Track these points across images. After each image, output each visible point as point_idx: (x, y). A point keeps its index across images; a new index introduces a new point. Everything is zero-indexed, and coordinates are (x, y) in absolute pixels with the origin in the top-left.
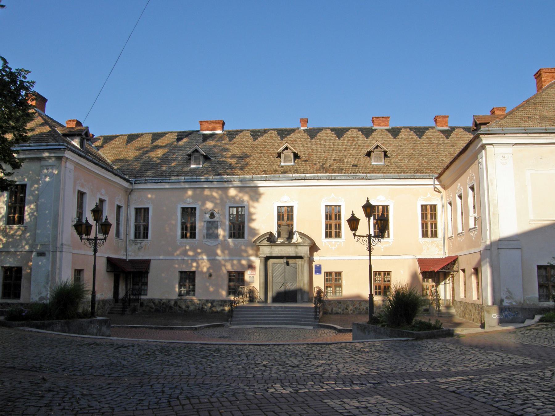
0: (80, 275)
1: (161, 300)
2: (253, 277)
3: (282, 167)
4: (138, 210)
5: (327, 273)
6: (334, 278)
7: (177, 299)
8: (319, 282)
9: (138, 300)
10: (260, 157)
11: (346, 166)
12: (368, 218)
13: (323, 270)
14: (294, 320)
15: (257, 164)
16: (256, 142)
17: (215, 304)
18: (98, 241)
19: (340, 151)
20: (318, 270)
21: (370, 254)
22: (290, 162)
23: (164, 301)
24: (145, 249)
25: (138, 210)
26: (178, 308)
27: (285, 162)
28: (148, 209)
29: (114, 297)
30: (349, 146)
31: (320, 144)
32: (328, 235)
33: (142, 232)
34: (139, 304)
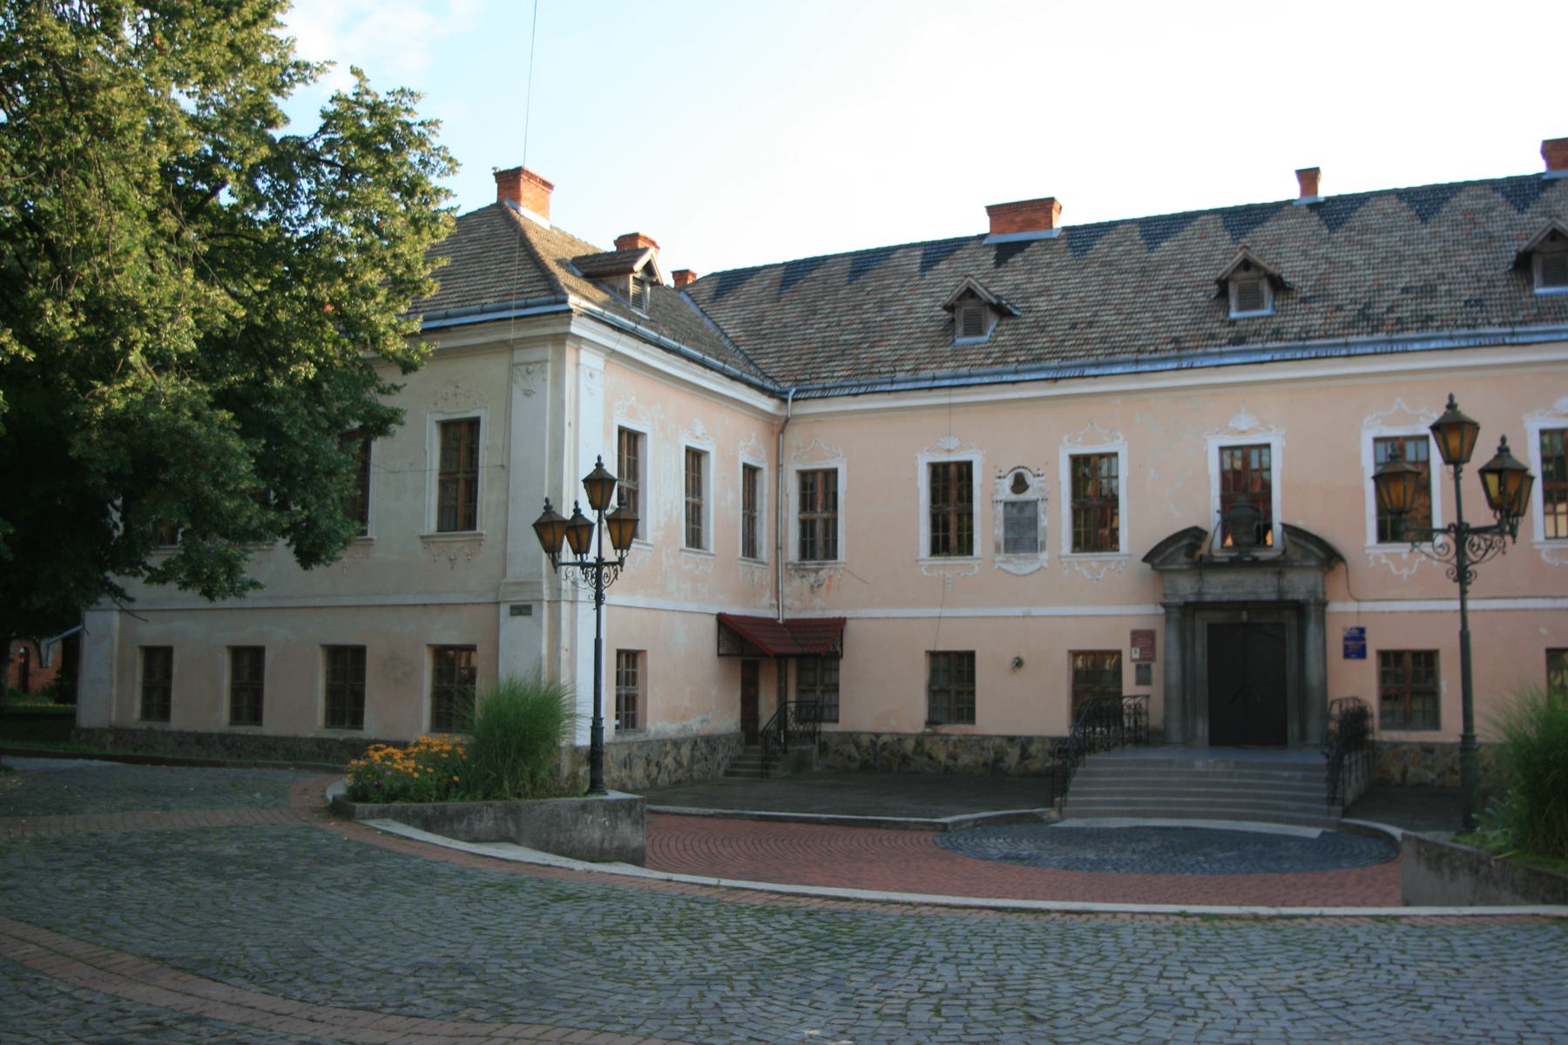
0: (634, 666)
1: (878, 735)
2: (1148, 668)
3: (1233, 323)
4: (807, 479)
5: (1384, 656)
6: (1410, 675)
7: (924, 734)
8: (1357, 683)
9: (812, 736)
10: (1164, 299)
11: (1440, 306)
12: (1451, 468)
13: (1373, 644)
14: (1262, 807)
15: (1157, 319)
16: (1155, 256)
17: (1033, 749)
18: (605, 570)
19: (1425, 261)
20: (1355, 646)
21: (1463, 593)
22: (1258, 305)
23: (885, 738)
24: (829, 587)
25: (807, 479)
26: (926, 759)
27: (1241, 309)
28: (835, 471)
29: (743, 728)
30: (1457, 242)
31: (1360, 243)
32: (1388, 532)
33: (818, 540)
34: (816, 748)
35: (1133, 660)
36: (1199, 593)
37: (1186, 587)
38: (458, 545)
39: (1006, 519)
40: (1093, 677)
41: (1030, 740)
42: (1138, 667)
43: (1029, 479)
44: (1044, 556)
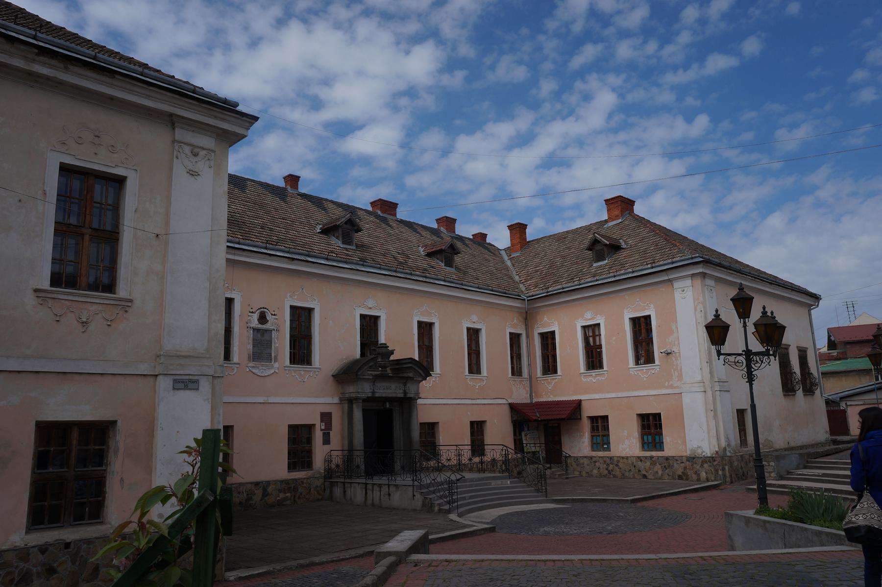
17: (269, 490)
35: (321, 430)
36: (373, 393)
37: (365, 389)
38: (95, 307)
39: (254, 339)
40: (299, 439)
41: (268, 483)
42: (324, 434)
43: (269, 317)
44: (276, 365)
